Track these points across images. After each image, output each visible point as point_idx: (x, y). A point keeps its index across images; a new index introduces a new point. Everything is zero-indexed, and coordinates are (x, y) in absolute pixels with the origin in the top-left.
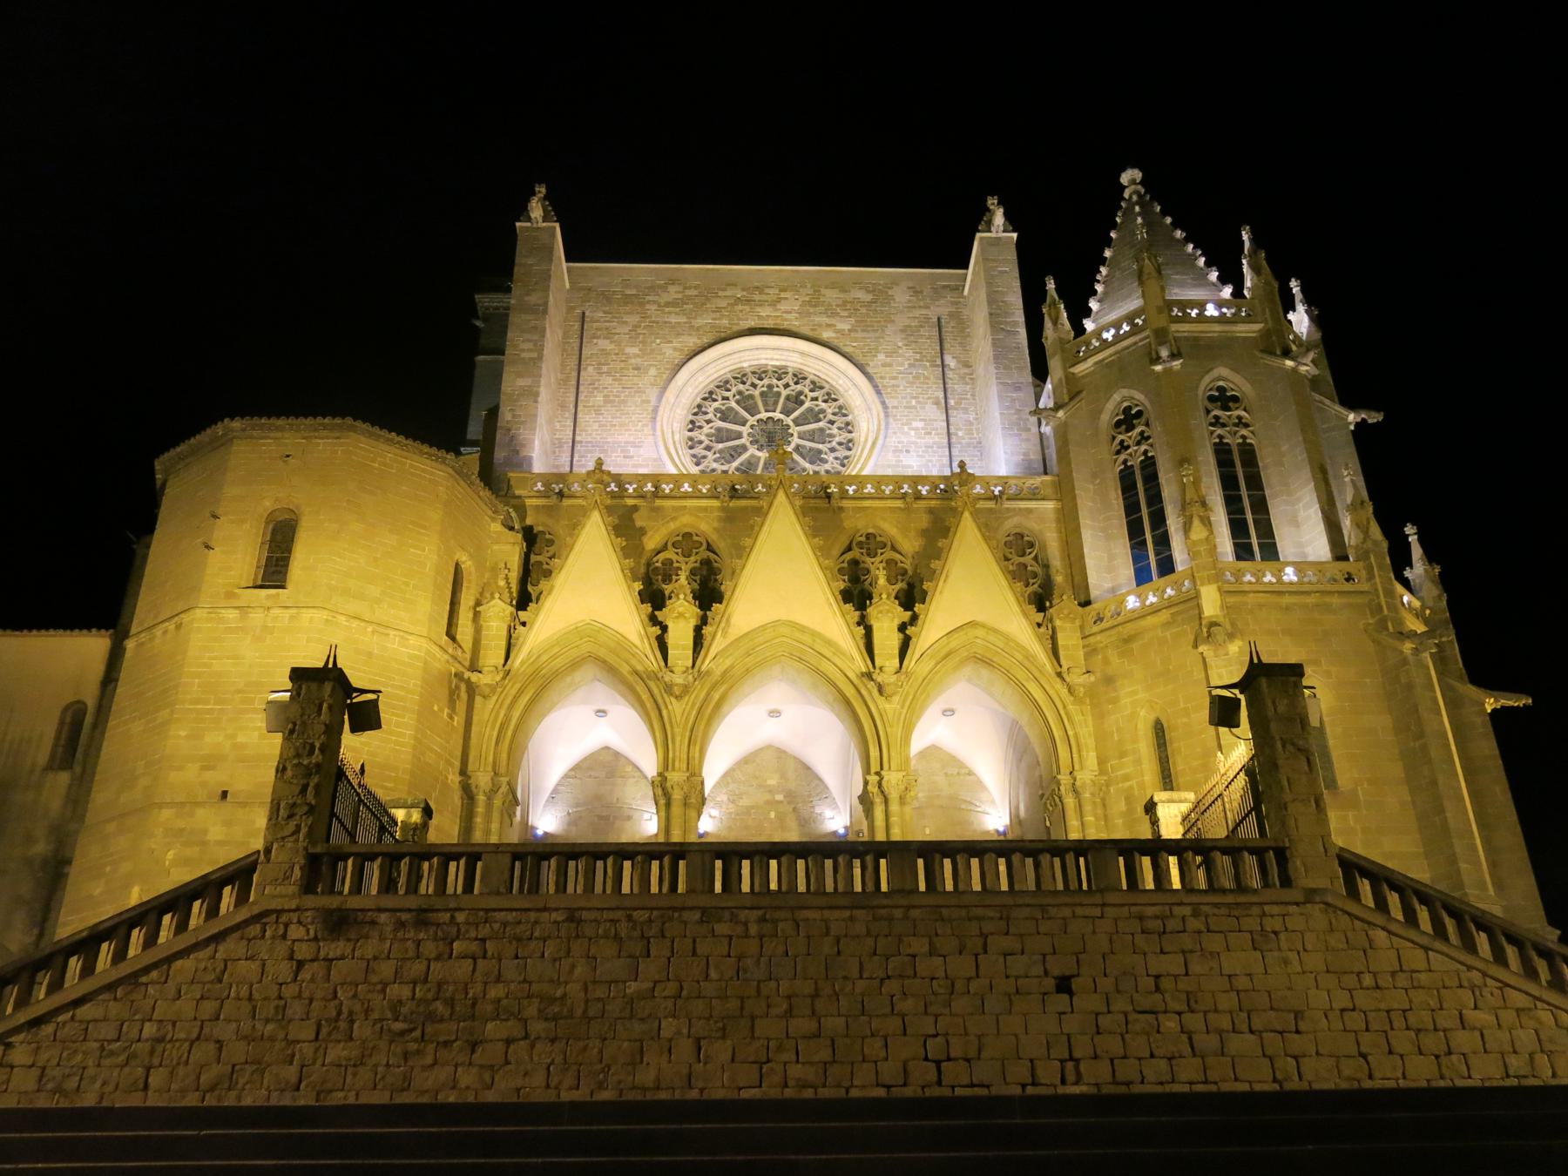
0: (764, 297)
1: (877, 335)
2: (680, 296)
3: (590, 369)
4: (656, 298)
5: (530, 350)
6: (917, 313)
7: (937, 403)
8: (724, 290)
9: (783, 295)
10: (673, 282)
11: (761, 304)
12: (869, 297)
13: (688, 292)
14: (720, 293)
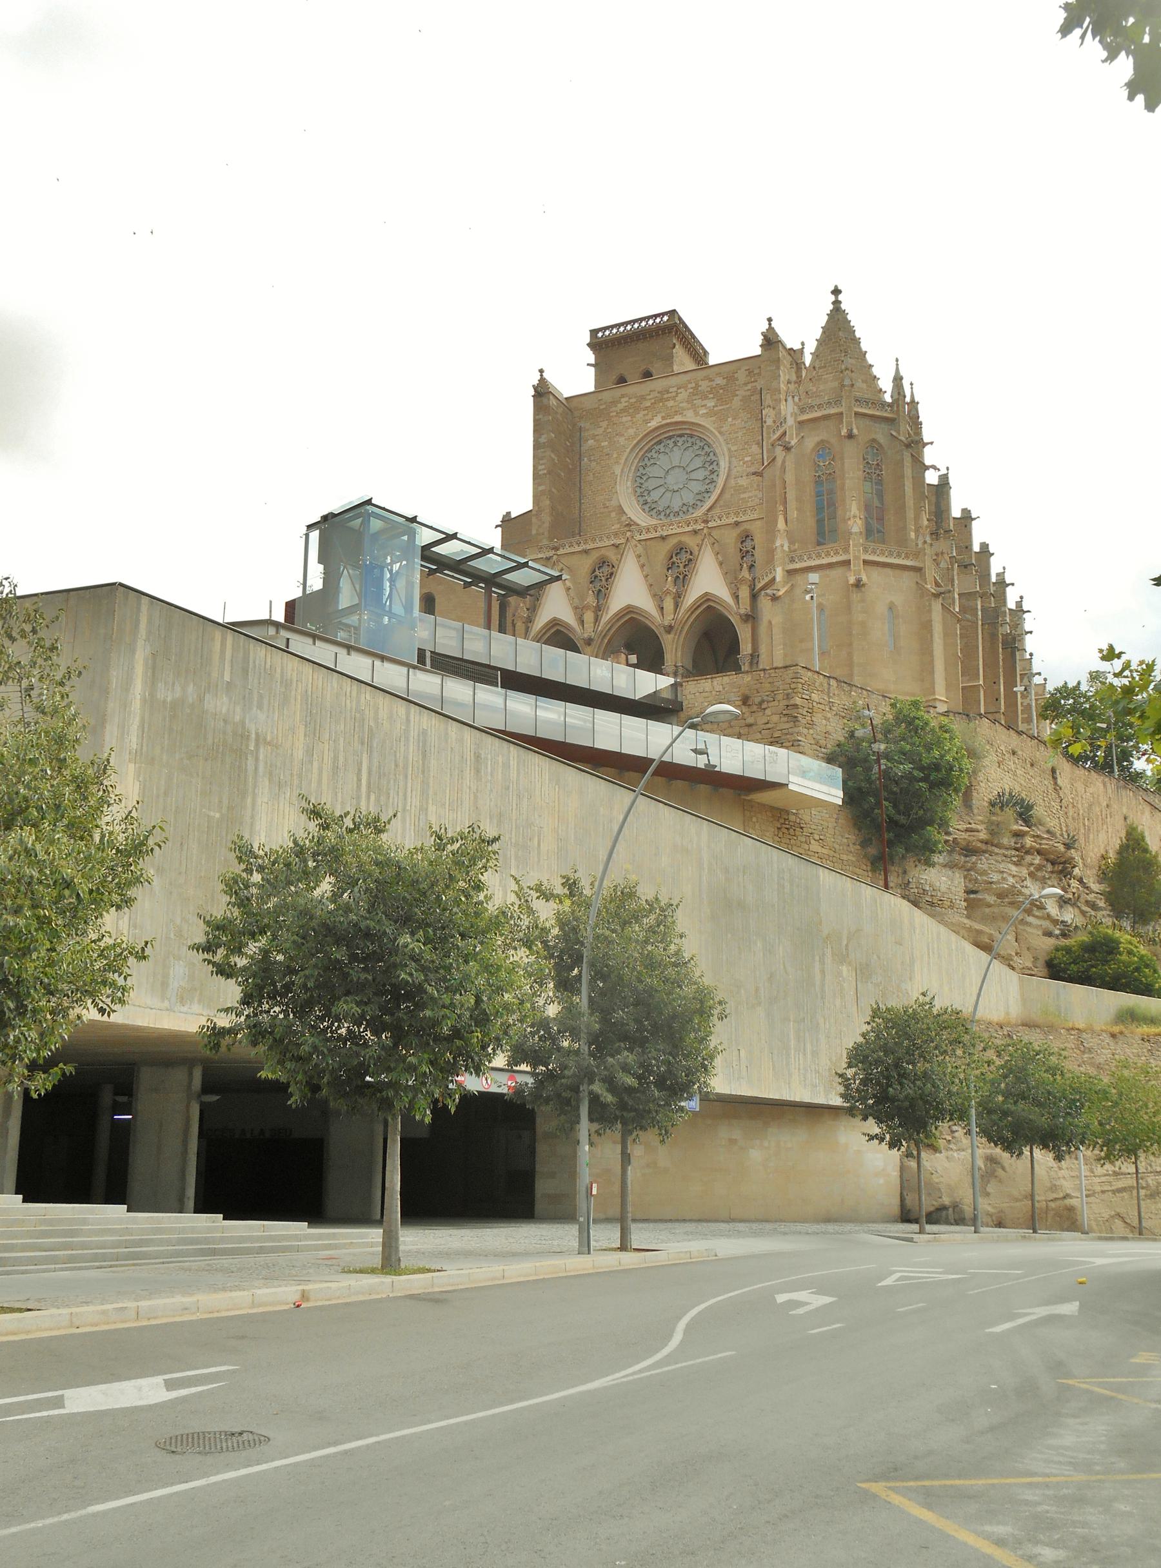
0: (669, 395)
2: (627, 404)
3: (586, 459)
4: (614, 409)
5: (543, 469)
6: (749, 387)
7: (758, 444)
8: (650, 394)
9: (679, 391)
10: (623, 396)
11: (668, 400)
13: (631, 401)
14: (648, 397)
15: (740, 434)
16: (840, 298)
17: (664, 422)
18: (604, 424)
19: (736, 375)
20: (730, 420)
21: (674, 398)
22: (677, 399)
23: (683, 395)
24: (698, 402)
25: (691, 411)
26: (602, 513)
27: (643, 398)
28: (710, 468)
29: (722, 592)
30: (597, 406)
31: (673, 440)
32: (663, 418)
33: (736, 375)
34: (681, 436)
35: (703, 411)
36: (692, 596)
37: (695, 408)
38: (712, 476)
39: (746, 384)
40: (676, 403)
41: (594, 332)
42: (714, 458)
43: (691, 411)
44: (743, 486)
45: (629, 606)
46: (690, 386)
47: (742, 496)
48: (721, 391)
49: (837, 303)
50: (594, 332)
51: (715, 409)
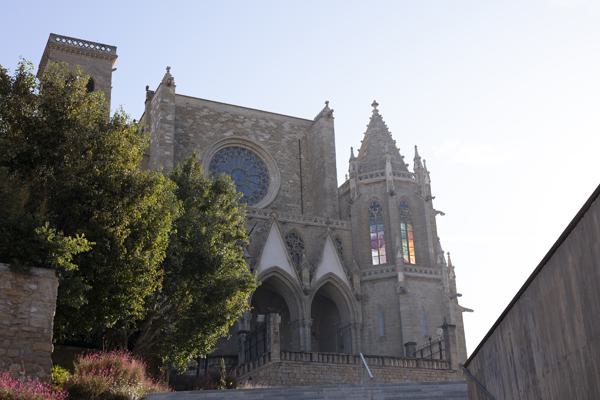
10: (205, 107)
11: (237, 122)
12: (275, 126)
16: (378, 108)
17: (235, 136)
21: (242, 123)
23: (248, 124)
24: (258, 132)
29: (341, 275)
34: (244, 149)
35: (262, 140)
36: (320, 274)
41: (53, 36)
45: (276, 267)
49: (376, 111)
50: (53, 36)
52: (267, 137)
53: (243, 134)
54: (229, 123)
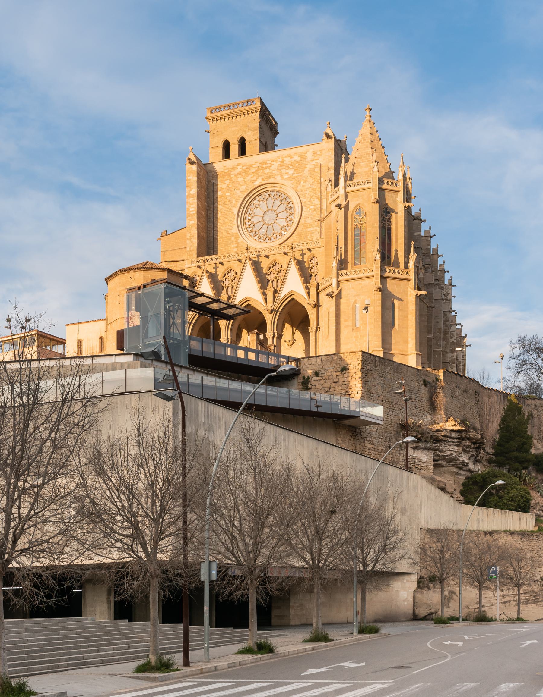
0: (267, 165)
1: (300, 174)
2: (241, 170)
6: (314, 163)
7: (318, 198)
8: (254, 164)
9: (273, 163)
10: (239, 165)
11: (265, 168)
14: (254, 166)
15: (308, 192)
18: (227, 182)
19: (306, 155)
20: (302, 182)
22: (271, 168)
23: (275, 166)
24: (284, 171)
25: (279, 176)
26: (227, 237)
27: (251, 166)
28: (290, 212)
30: (222, 170)
31: (268, 193)
32: (263, 180)
33: (306, 155)
34: (273, 191)
36: (283, 294)
37: (282, 175)
38: (291, 217)
39: (312, 161)
40: (271, 171)
42: (292, 206)
43: (279, 176)
44: (309, 223)
46: (279, 160)
47: (308, 230)
48: (297, 165)
51: (294, 175)
52: (291, 172)
53: (271, 177)
54: (259, 171)
